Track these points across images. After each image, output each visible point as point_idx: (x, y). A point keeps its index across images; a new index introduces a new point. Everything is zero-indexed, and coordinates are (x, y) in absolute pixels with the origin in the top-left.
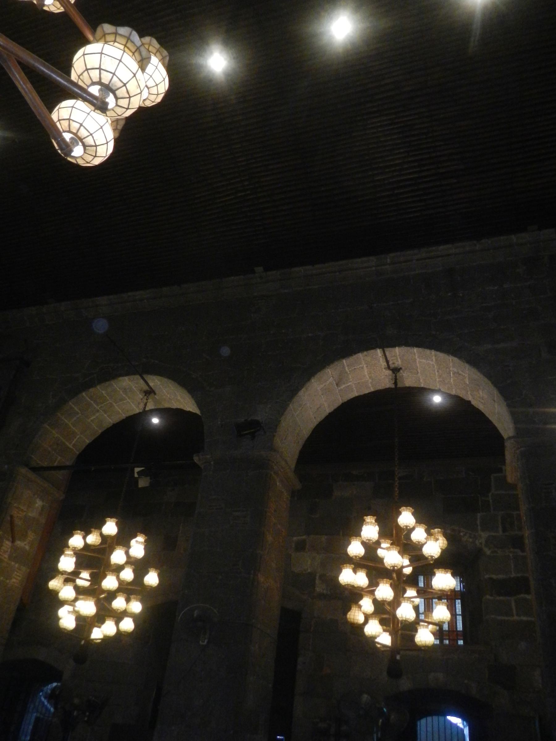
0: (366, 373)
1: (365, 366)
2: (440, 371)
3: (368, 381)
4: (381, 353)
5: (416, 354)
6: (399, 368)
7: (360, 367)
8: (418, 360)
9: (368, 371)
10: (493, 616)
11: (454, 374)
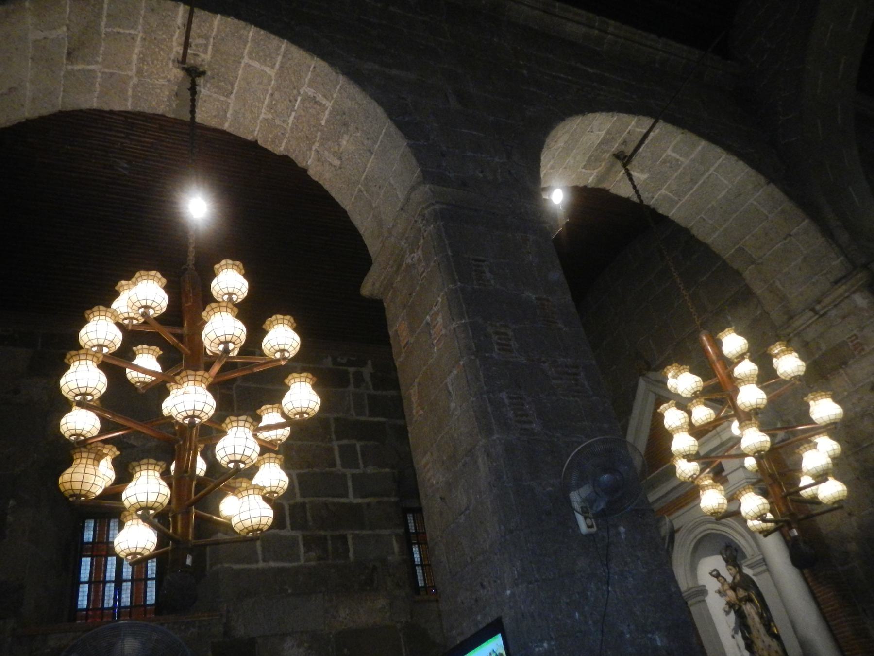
0: (135, 57)
1: (141, 35)
2: (277, 95)
3: (131, 77)
4: (183, 16)
5: (249, 45)
6: (201, 70)
7: (130, 34)
8: (246, 60)
9: (141, 52)
10: (226, 565)
11: (303, 102)
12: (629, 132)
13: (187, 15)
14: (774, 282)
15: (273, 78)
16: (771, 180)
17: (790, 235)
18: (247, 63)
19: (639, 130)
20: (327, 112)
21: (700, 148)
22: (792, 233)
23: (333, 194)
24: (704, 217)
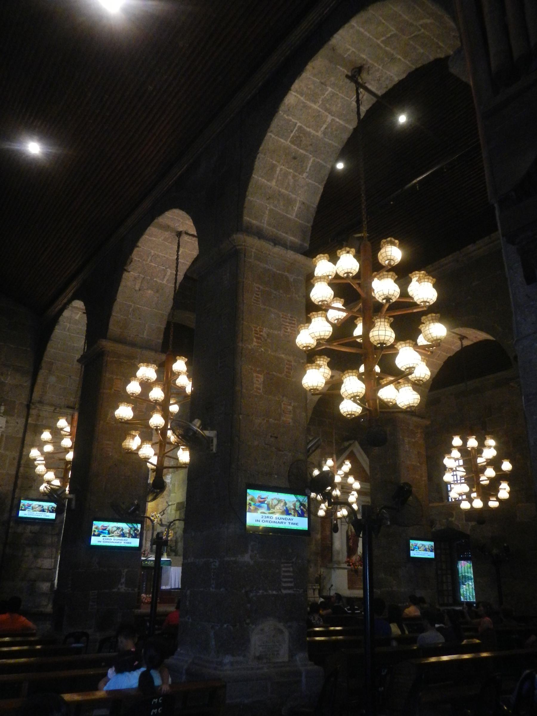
11: (163, 270)
14: (48, 384)
17: (70, 376)
20: (161, 281)
23: (121, 288)
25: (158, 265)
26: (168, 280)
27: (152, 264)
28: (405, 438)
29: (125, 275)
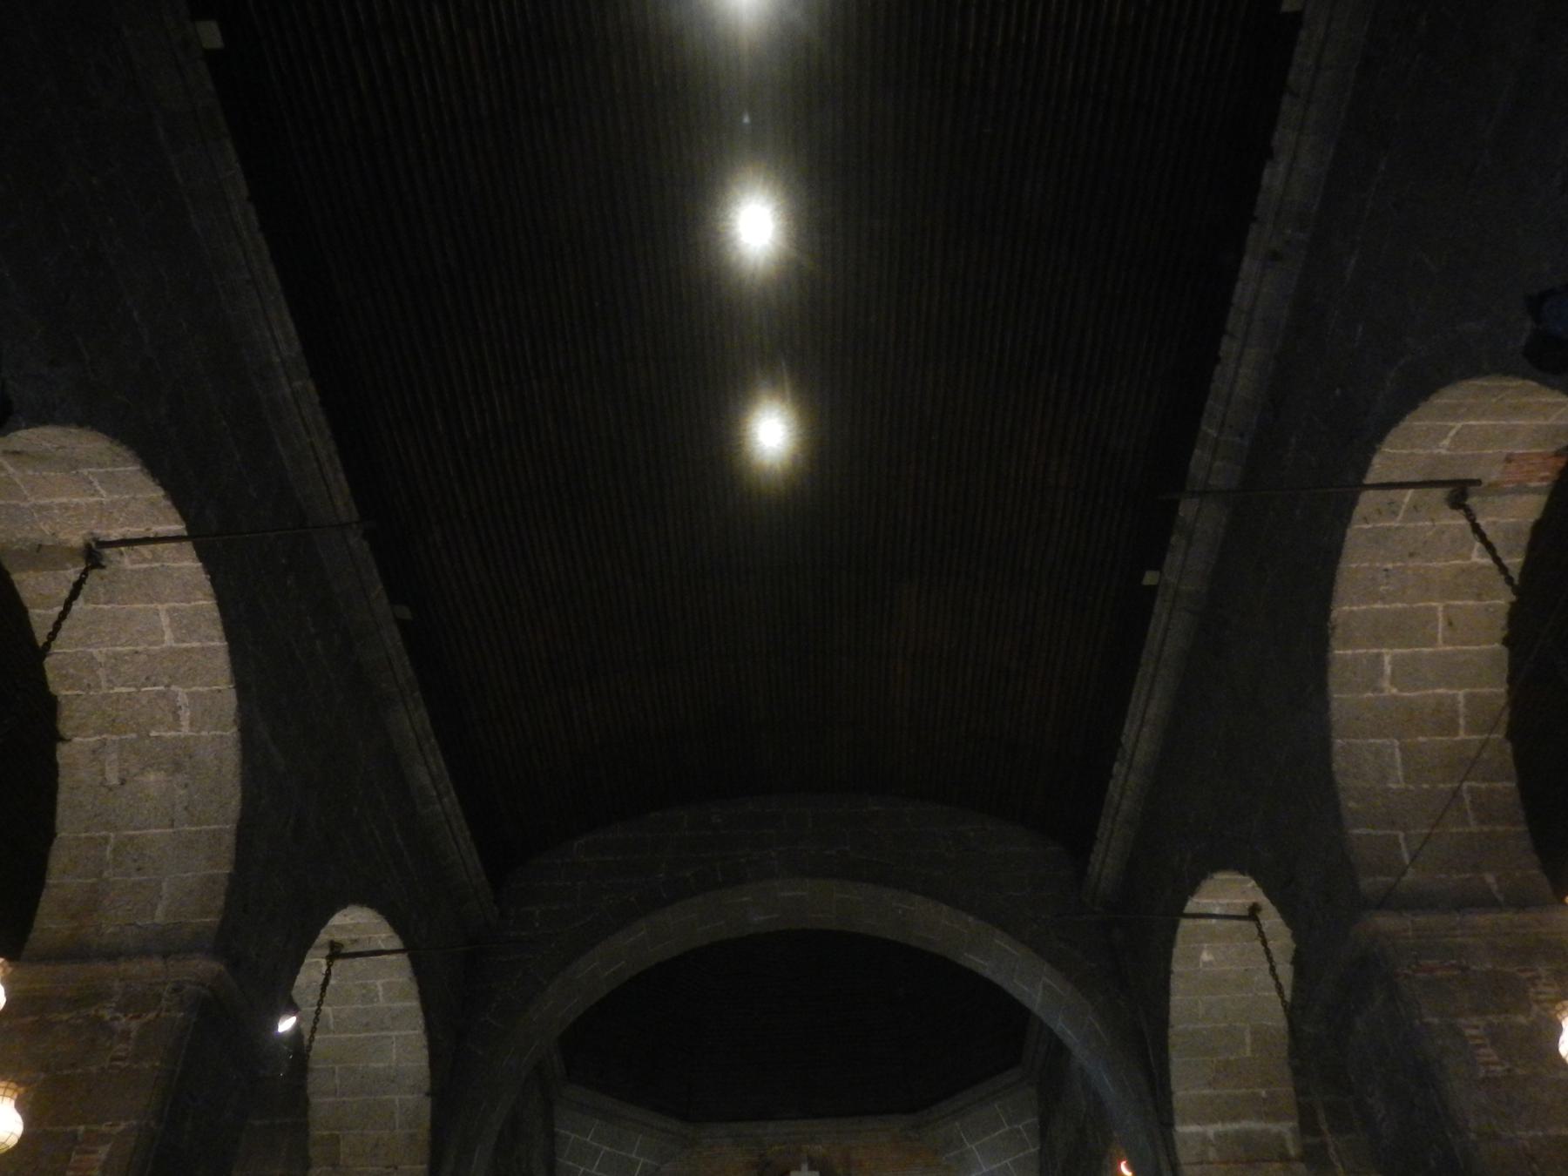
6: (104, 563)
11: (162, 695)
12: (370, 938)
13: (172, 534)
15: (164, 645)
16: (431, 1094)
17: (396, 1168)
18: (157, 610)
19: (380, 942)
20: (173, 733)
21: (408, 1004)
22: (399, 1167)
23: (63, 796)
24: (337, 1071)
25: (136, 686)
26: (191, 724)
27: (117, 690)
28: (1462, 1021)
29: (63, 752)
